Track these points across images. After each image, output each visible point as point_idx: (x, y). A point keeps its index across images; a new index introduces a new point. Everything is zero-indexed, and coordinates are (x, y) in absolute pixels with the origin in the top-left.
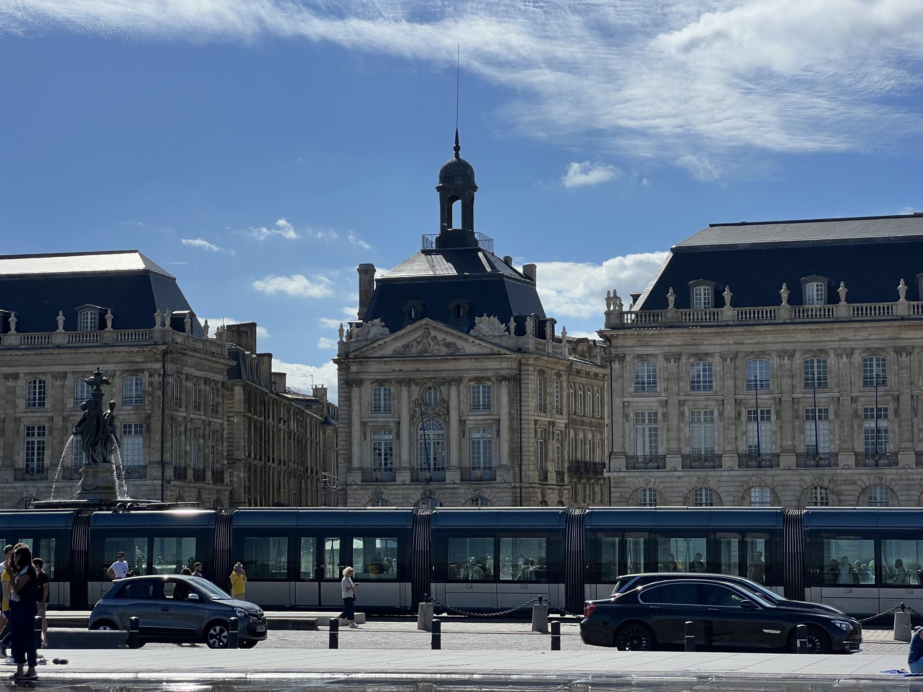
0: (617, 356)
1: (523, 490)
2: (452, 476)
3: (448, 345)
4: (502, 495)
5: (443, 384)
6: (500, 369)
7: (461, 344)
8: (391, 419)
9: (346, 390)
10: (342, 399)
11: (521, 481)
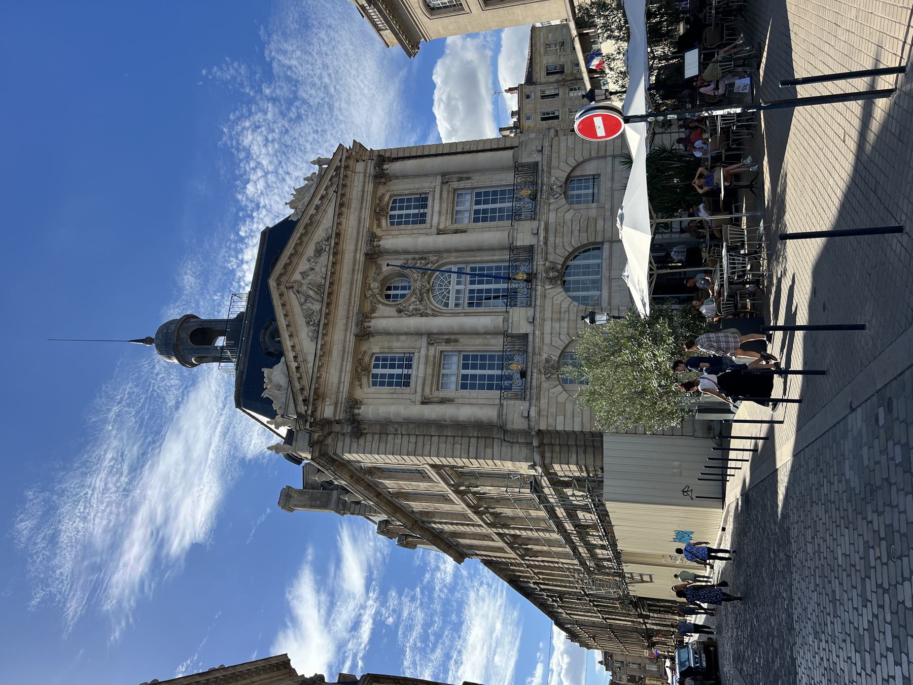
2: (524, 235)
3: (319, 252)
4: (563, 151)
5: (379, 267)
6: (365, 173)
7: (320, 234)
8: (423, 352)
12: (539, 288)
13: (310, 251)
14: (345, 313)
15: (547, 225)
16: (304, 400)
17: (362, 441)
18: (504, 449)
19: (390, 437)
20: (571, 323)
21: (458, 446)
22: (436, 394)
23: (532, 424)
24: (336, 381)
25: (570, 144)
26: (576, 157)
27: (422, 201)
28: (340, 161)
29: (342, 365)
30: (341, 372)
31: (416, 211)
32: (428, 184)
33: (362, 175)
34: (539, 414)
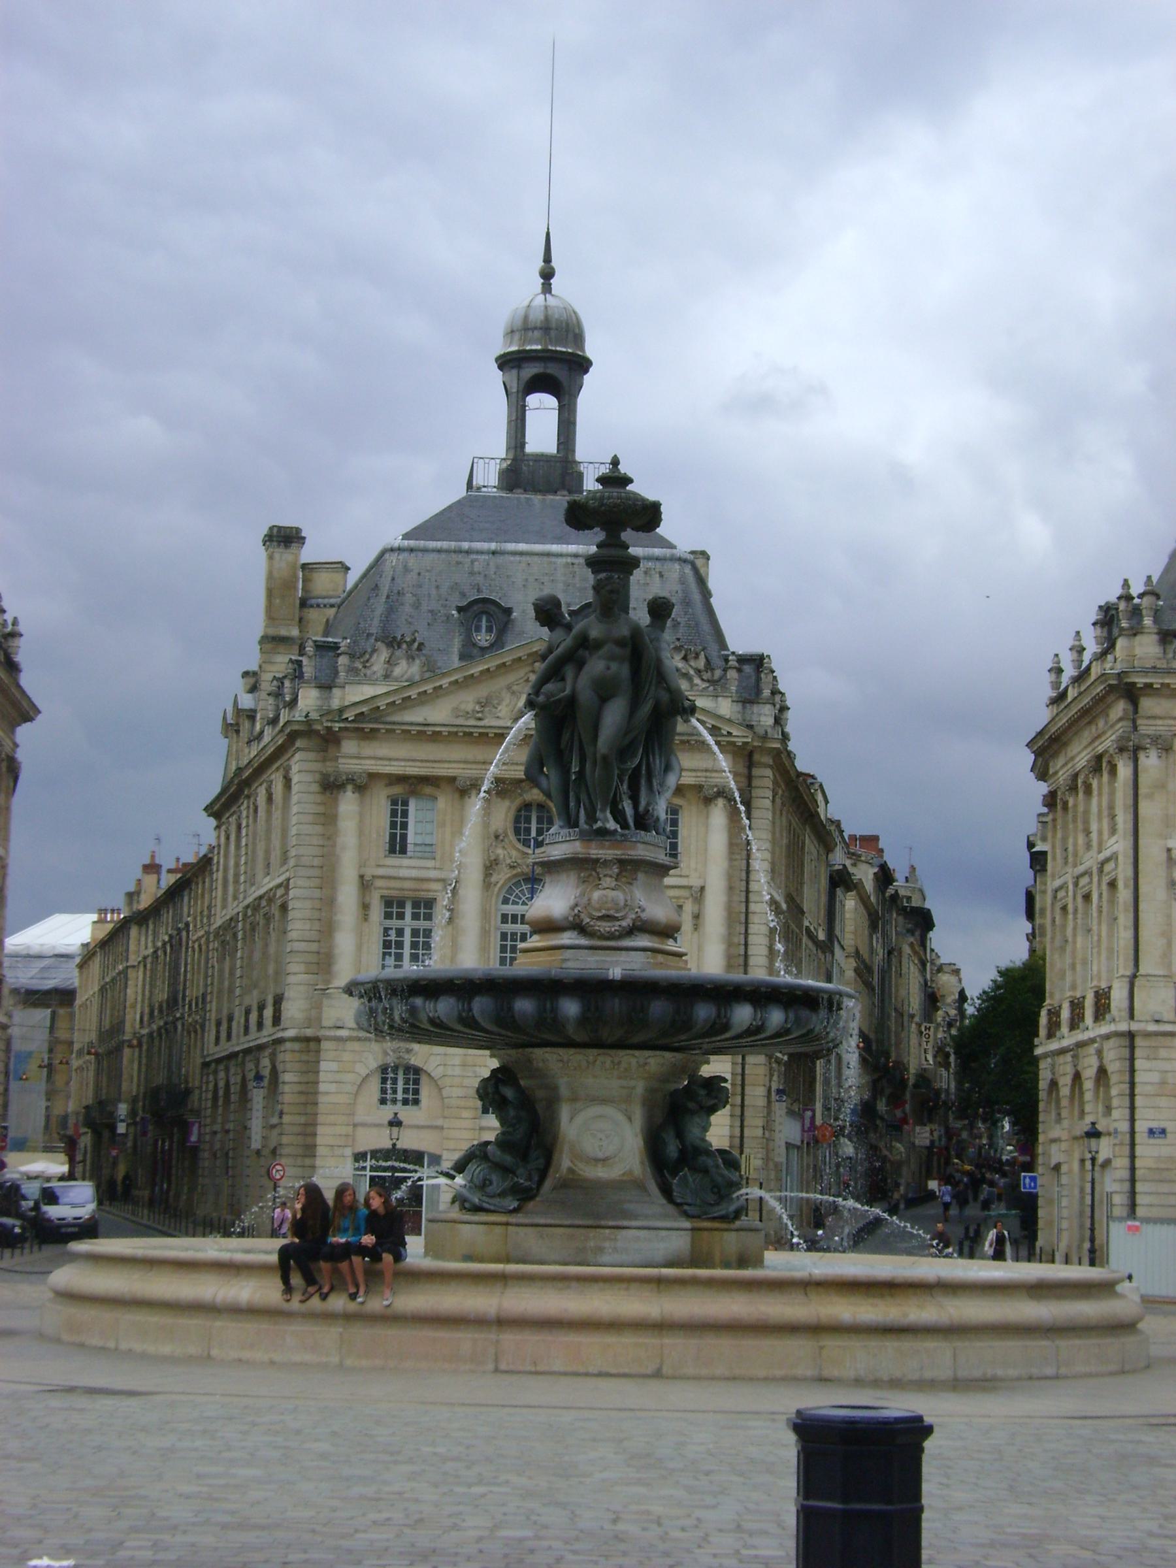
0: (1156, 740)
9: (319, 798)
10: (310, 818)
17: (315, 787)
19: (319, 829)
32: (693, 865)
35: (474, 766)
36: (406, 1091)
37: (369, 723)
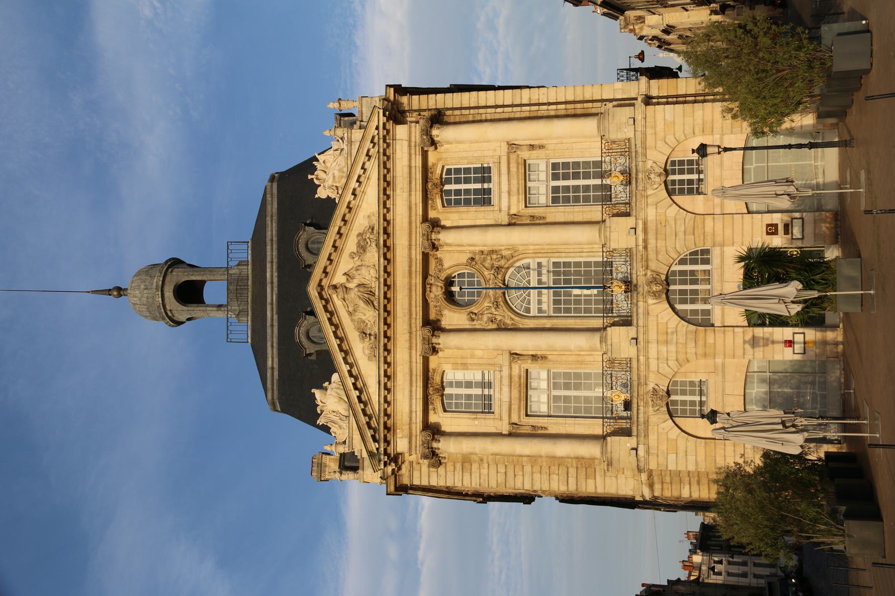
1: (654, 93)
3: (362, 248)
4: (660, 126)
6: (410, 141)
9: (450, 467)
11: (636, 99)
12: (641, 304)
13: (351, 244)
14: (406, 327)
15: (645, 224)
16: (373, 437)
17: (441, 470)
18: (608, 480)
19: (475, 467)
20: (680, 346)
21: (555, 477)
22: (525, 420)
23: (642, 464)
24: (406, 409)
25: (669, 117)
26: (677, 135)
27: (484, 174)
28: (377, 128)
29: (411, 391)
30: (411, 399)
31: (478, 186)
32: (491, 153)
33: (406, 144)
34: (648, 452)
35: (414, 341)
36: (692, 393)
37: (380, 429)
